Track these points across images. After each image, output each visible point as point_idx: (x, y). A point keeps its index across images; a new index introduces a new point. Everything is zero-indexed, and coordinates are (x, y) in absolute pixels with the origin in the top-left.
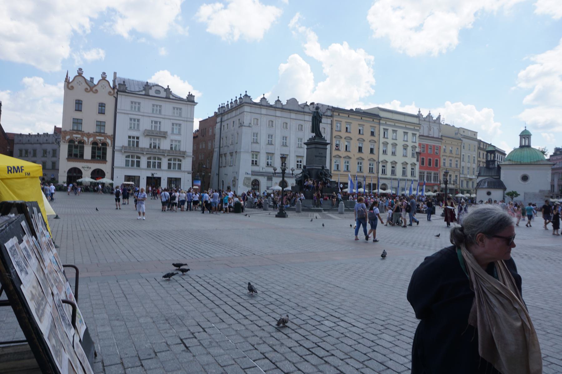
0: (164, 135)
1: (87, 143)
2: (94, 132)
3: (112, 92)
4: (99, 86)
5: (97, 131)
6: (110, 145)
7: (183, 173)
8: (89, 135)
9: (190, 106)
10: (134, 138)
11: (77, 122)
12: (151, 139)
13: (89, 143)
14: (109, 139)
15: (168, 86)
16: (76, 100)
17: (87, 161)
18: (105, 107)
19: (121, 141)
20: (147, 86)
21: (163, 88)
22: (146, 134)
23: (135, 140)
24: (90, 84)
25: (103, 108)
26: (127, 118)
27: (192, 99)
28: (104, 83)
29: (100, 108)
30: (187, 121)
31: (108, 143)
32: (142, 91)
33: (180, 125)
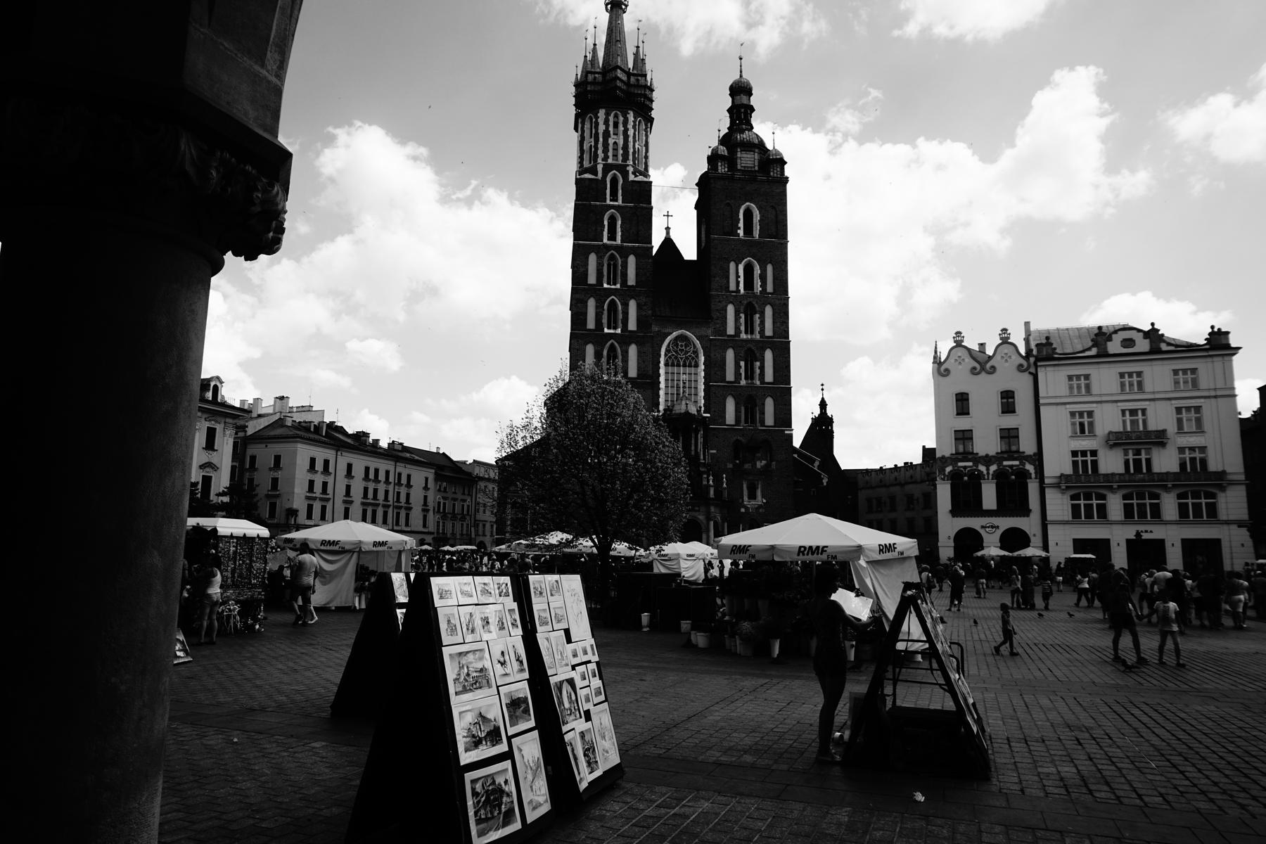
0: (1159, 439)
1: (986, 477)
2: (997, 453)
3: (1025, 363)
4: (998, 357)
5: (1004, 449)
6: (1033, 476)
7: (1225, 527)
8: (987, 460)
9: (1220, 358)
10: (1084, 453)
11: (964, 437)
12: (1126, 454)
13: (990, 477)
14: (1030, 463)
15: (1153, 324)
16: (956, 395)
17: (989, 513)
18: (1013, 397)
19: (1057, 463)
20: (1101, 336)
21: (1139, 331)
22: (1111, 443)
23: (1089, 458)
24: (981, 357)
25: (1010, 400)
26: (1064, 412)
27: (1224, 342)
28: (1006, 349)
29: (1005, 400)
30: (1216, 397)
31: (1028, 471)
32: (1089, 349)
33: (1198, 409)
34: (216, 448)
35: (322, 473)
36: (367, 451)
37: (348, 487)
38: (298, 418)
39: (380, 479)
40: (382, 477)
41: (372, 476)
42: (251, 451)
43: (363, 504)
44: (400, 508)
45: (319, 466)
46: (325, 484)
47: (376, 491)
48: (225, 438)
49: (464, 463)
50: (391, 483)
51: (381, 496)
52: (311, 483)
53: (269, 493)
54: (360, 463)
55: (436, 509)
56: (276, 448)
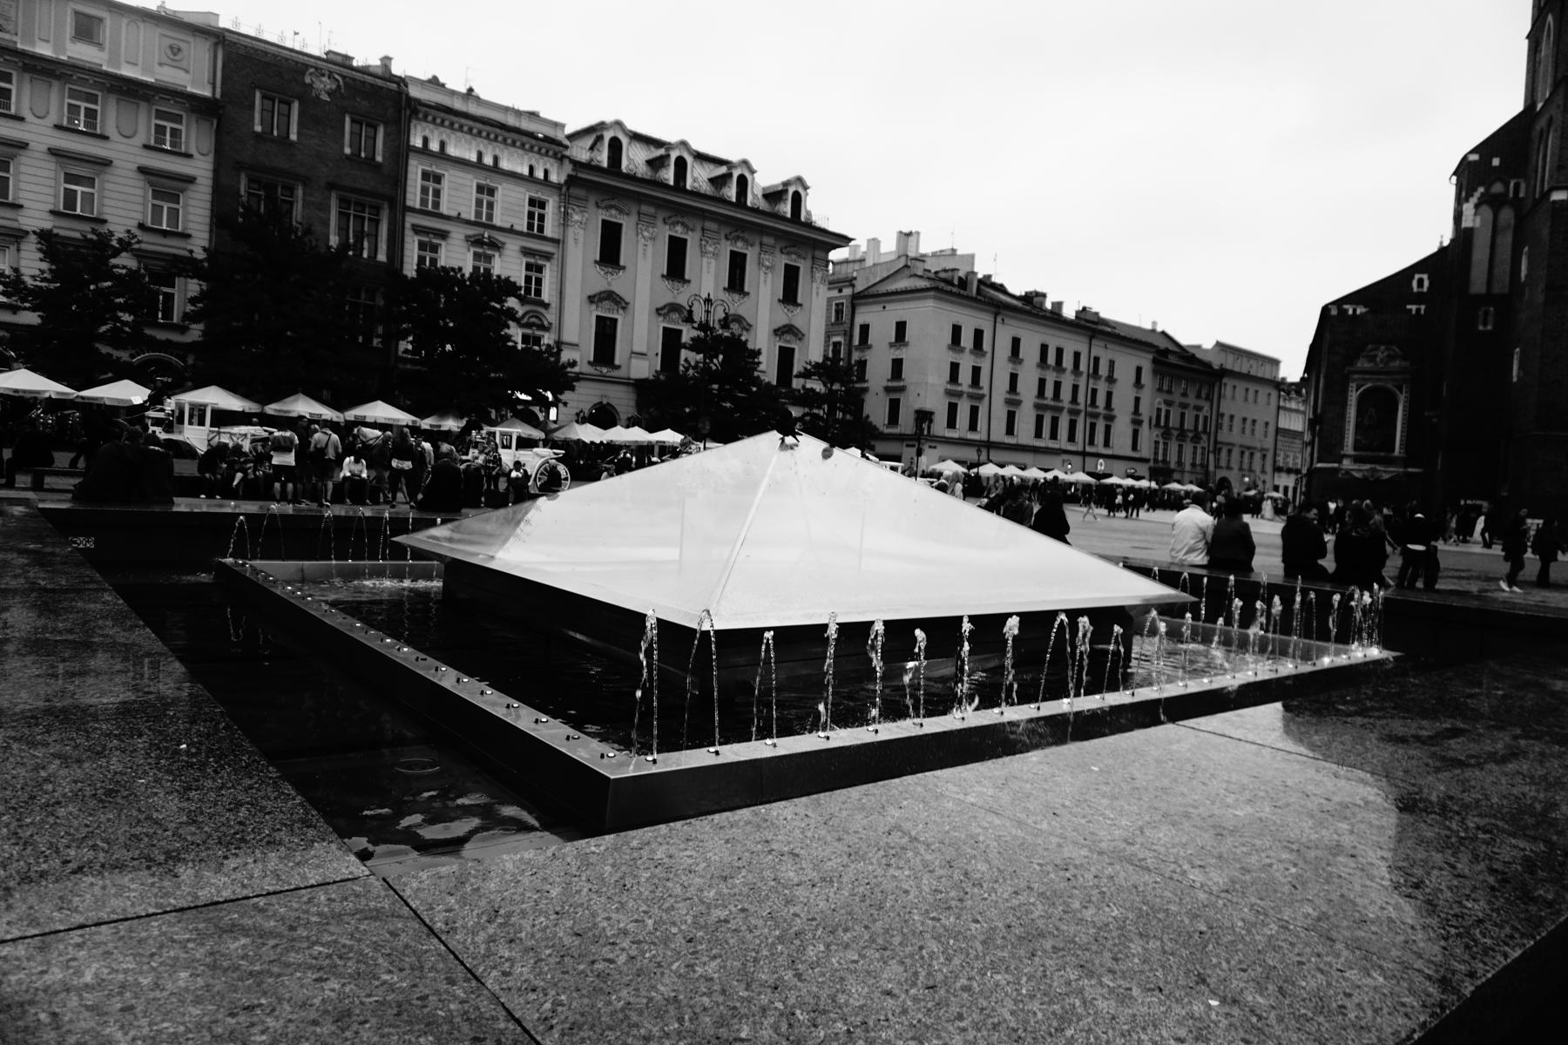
34: (799, 301)
35: (971, 352)
36: (1044, 317)
37: (1014, 378)
38: (934, 266)
39: (1064, 365)
40: (1068, 362)
41: (1051, 360)
42: (860, 320)
43: (1037, 406)
44: (1096, 416)
45: (967, 340)
46: (976, 371)
47: (1057, 385)
48: (815, 285)
49: (1199, 347)
50: (1081, 373)
51: (1066, 394)
52: (955, 368)
53: (890, 384)
54: (1032, 338)
55: (1154, 422)
56: (898, 311)
